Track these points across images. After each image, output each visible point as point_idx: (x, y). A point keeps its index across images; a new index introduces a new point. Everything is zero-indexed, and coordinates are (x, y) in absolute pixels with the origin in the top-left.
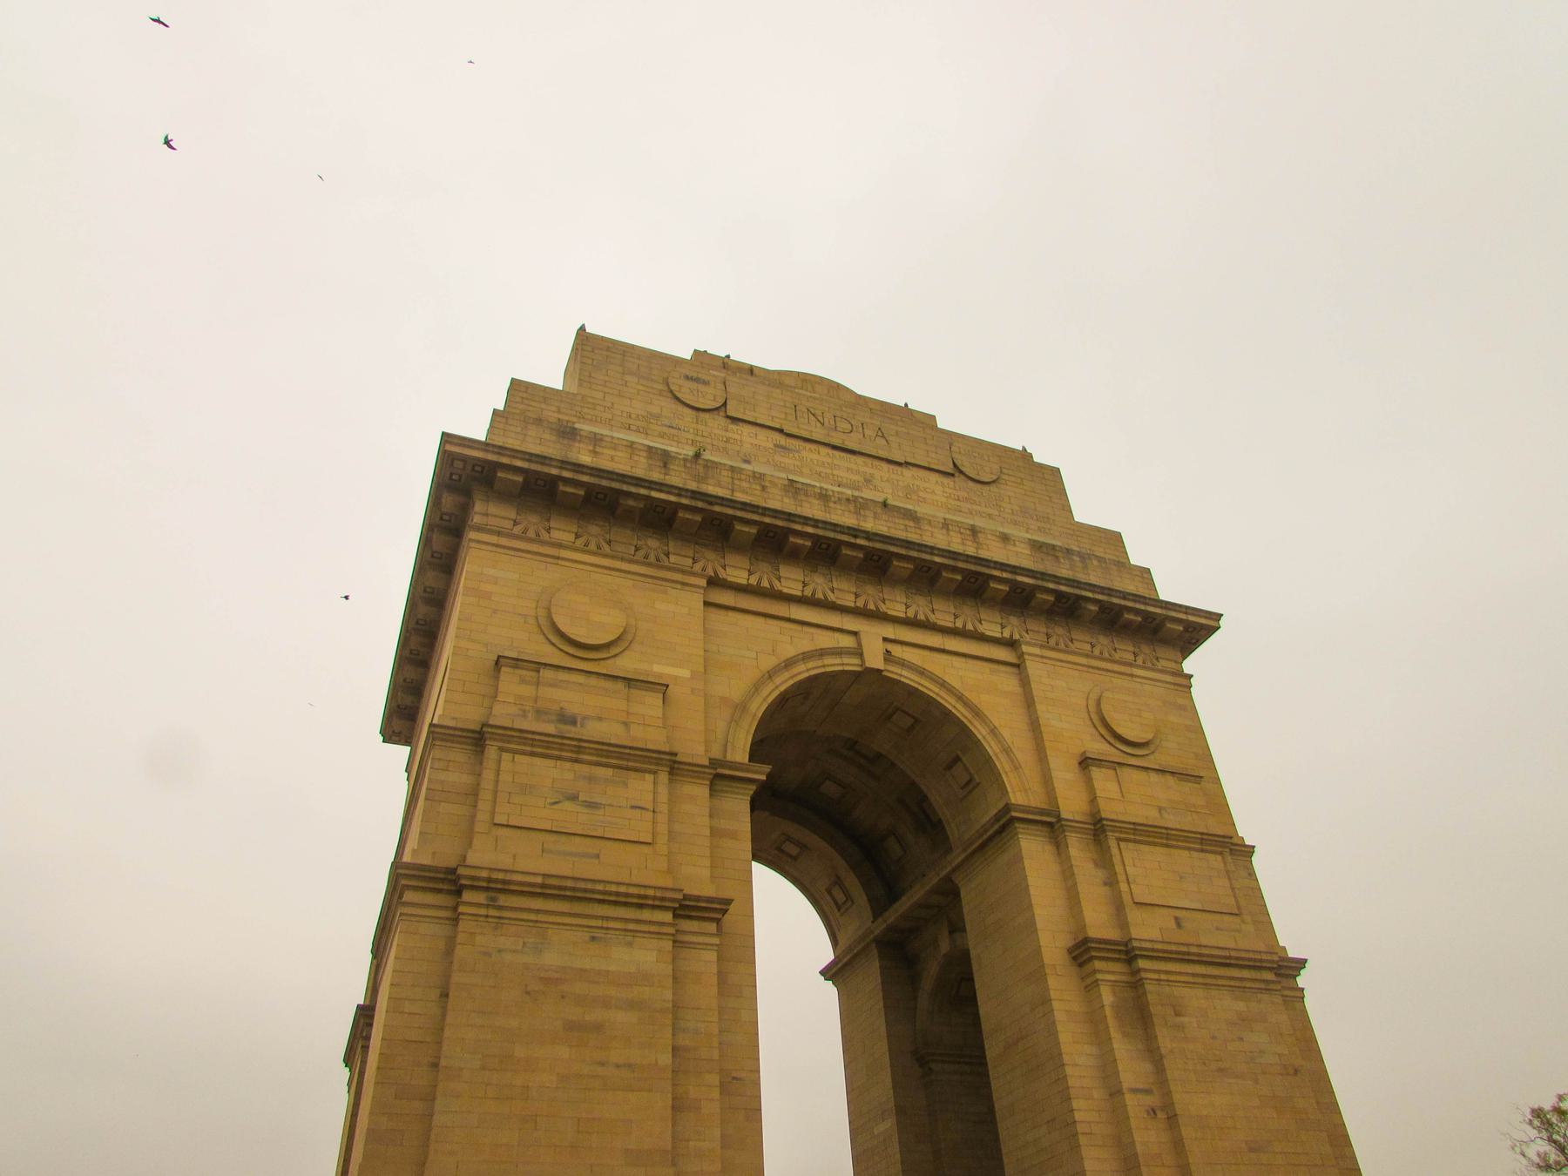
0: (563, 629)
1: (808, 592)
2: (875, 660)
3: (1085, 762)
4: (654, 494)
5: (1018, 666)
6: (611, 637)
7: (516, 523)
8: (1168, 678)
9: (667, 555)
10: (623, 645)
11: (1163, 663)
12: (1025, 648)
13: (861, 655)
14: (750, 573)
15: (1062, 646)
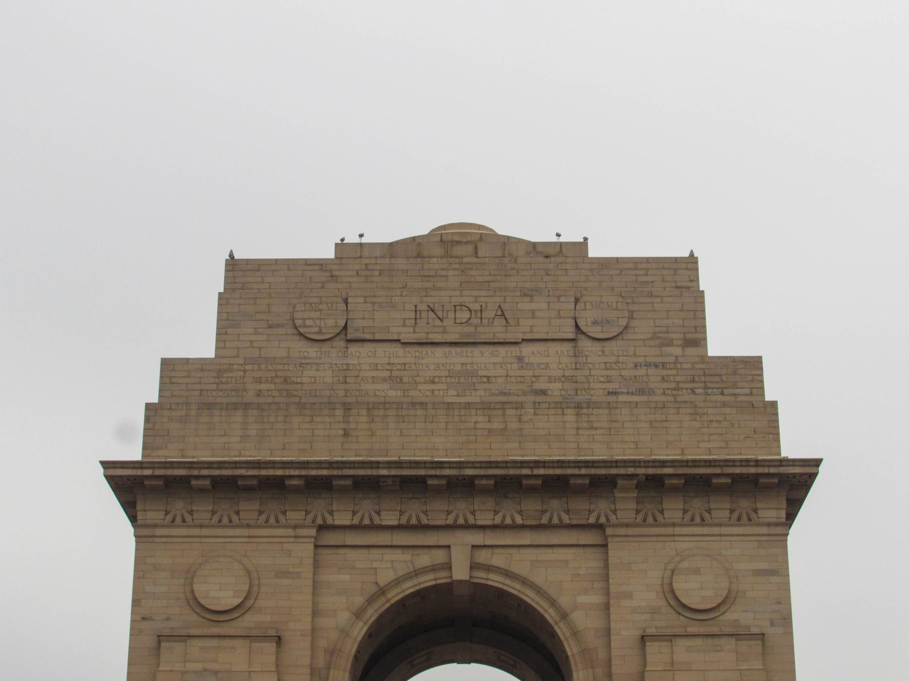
0: (202, 602)
1: (404, 521)
2: (460, 573)
3: (643, 639)
4: (264, 472)
5: (606, 546)
6: (237, 601)
7: (167, 513)
8: (764, 530)
9: (284, 513)
10: (250, 603)
11: (761, 513)
12: (609, 531)
13: (451, 568)
14: (354, 513)
15: (650, 520)
